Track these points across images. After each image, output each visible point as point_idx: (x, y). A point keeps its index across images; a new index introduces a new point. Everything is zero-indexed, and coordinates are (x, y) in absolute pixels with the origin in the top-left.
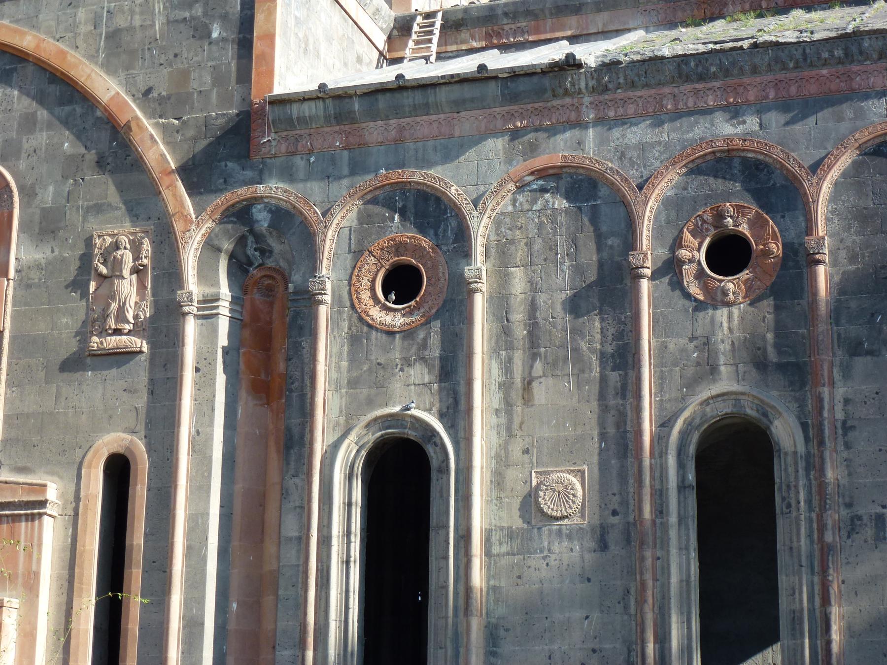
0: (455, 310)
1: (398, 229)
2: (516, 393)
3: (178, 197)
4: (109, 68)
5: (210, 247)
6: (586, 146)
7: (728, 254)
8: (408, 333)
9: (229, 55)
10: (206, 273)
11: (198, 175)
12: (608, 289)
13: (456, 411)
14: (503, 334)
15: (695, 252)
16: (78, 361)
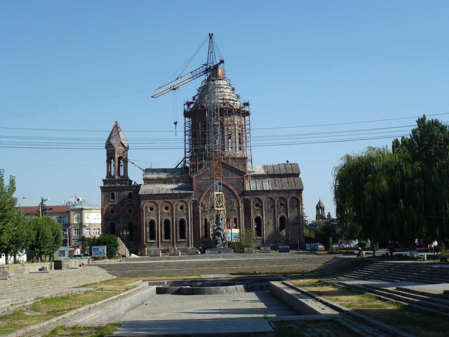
0: (262, 207)
1: (257, 201)
2: (266, 214)
3: (239, 197)
4: (231, 186)
5: (241, 202)
6: (271, 196)
7: (282, 205)
8: (258, 209)
9: (242, 186)
10: (241, 204)
11: (240, 196)
12: (273, 207)
13: (262, 216)
14: (265, 210)
15: (279, 204)
16: (231, 210)
